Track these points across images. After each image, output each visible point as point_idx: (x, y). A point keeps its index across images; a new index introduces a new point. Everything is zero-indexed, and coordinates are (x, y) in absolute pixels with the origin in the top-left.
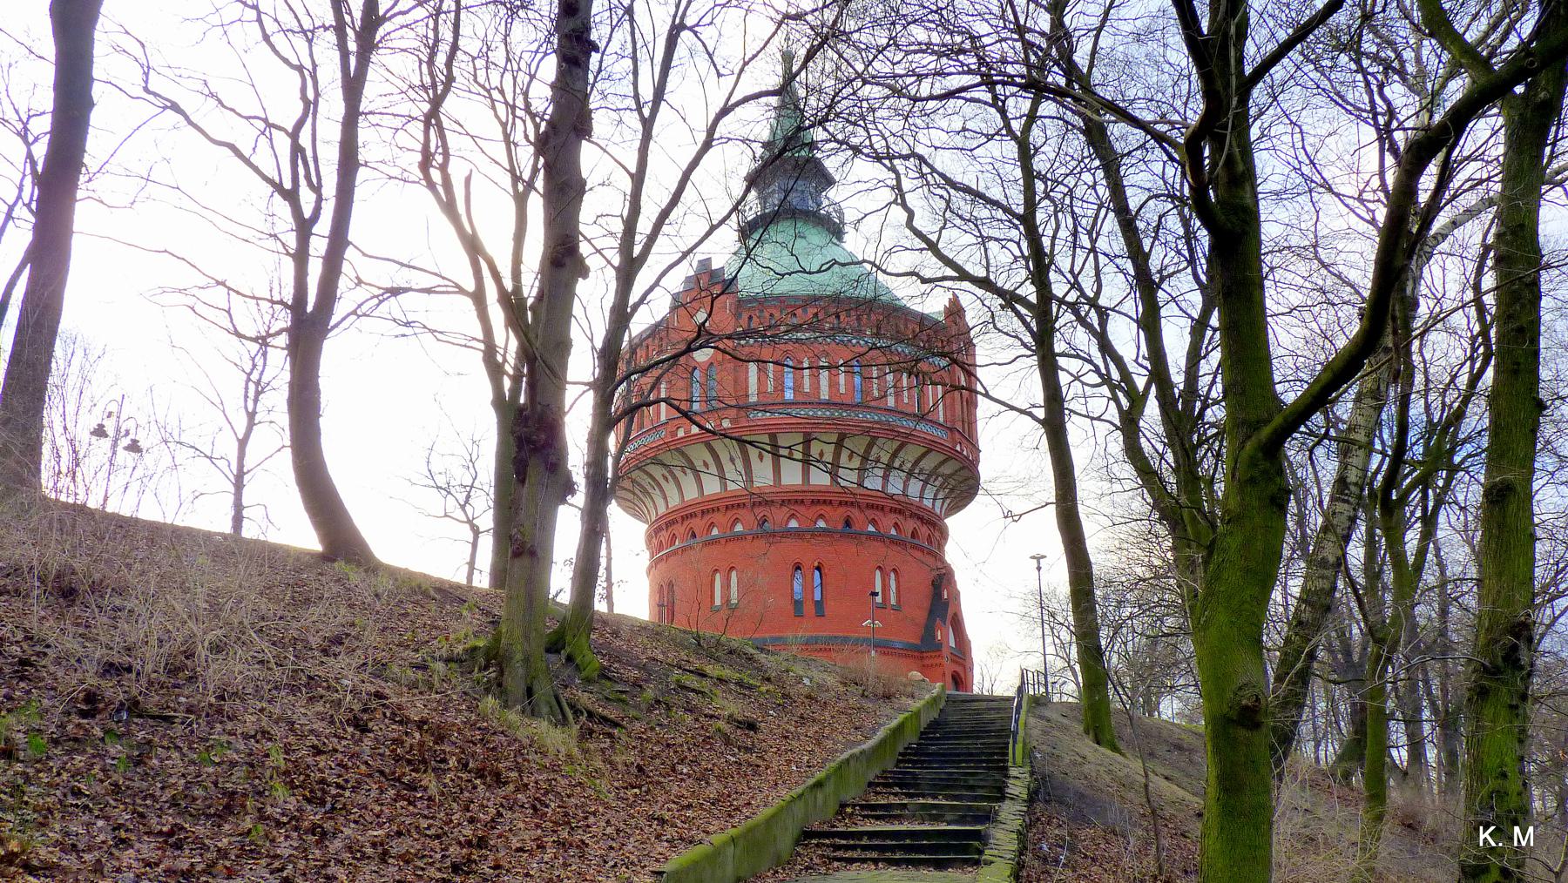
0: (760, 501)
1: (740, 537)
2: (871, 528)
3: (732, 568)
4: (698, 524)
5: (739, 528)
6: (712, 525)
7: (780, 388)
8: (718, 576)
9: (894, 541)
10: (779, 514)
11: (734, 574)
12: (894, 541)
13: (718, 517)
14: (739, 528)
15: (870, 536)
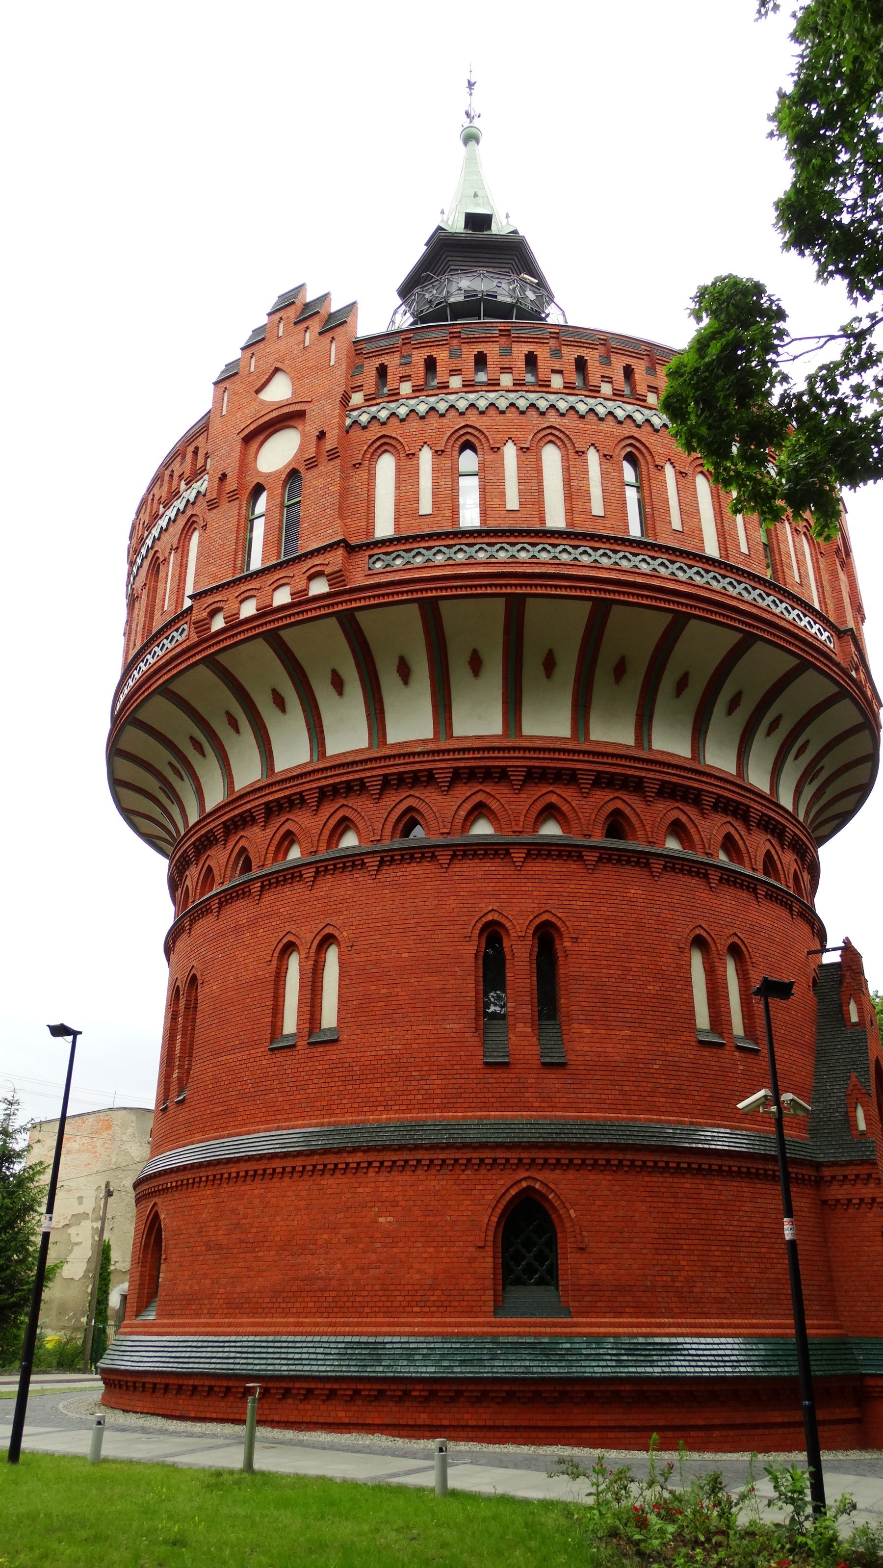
0: (399, 774)
1: (352, 862)
2: (672, 845)
3: (327, 940)
4: (257, 838)
5: (350, 841)
6: (289, 839)
7: (448, 499)
8: (294, 963)
9: (730, 878)
10: (440, 807)
11: (332, 956)
12: (730, 878)
13: (303, 821)
14: (350, 841)
15: (672, 863)
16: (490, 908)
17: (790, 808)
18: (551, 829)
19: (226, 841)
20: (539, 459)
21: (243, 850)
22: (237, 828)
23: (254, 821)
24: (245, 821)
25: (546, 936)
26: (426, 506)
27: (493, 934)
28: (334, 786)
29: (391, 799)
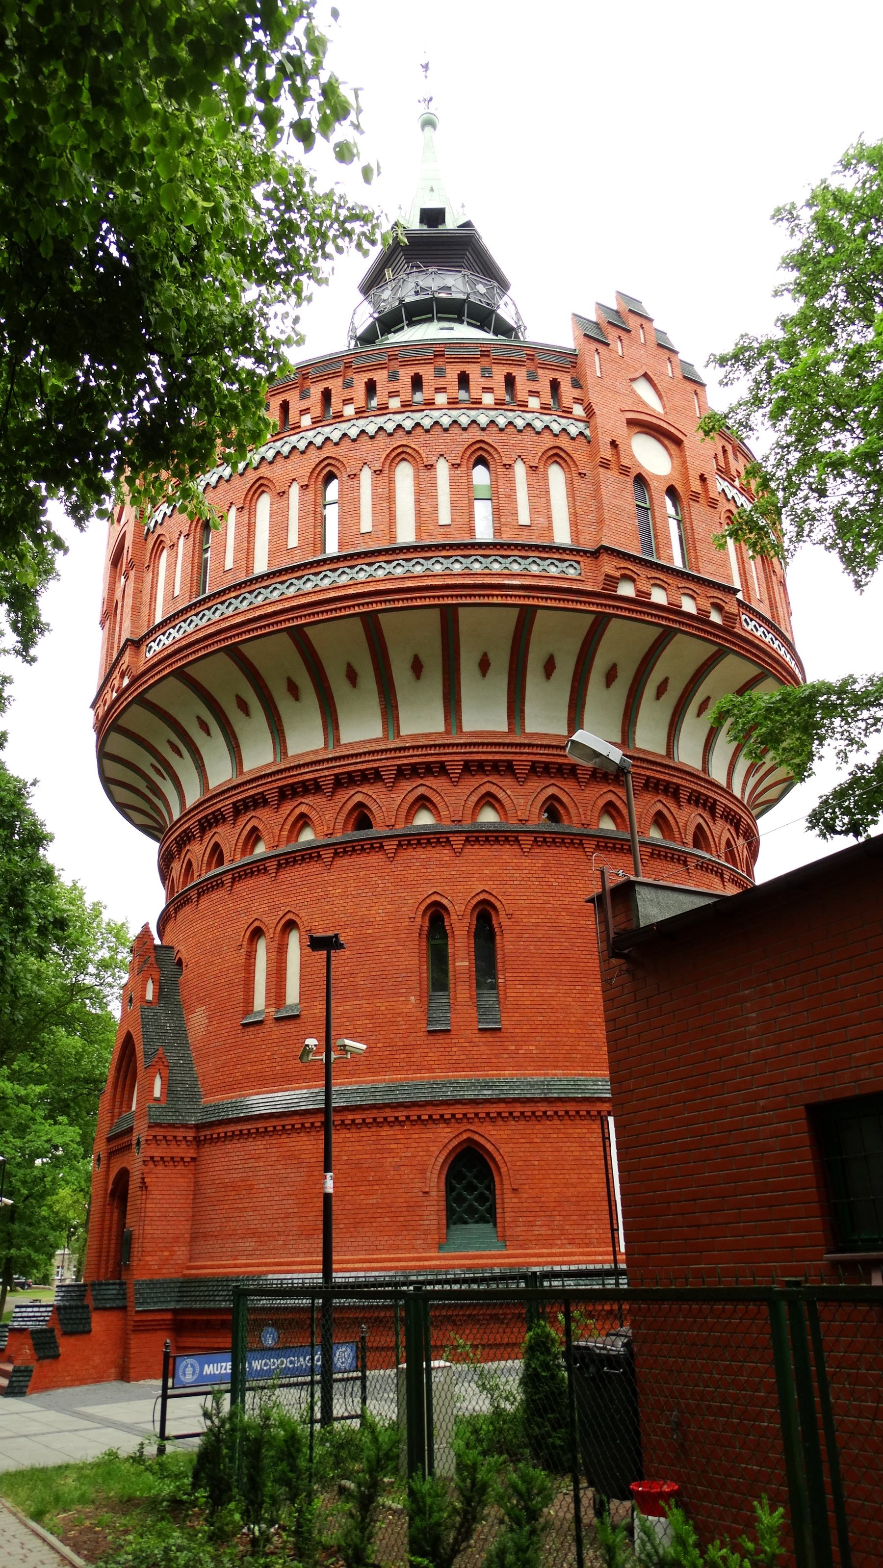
13: (267, 819)
16: (434, 890)
17: (723, 783)
18: (489, 816)
19: (202, 837)
20: (391, 481)
21: (217, 846)
22: (210, 826)
23: (224, 819)
24: (217, 819)
25: (485, 915)
26: (293, 541)
27: (436, 915)
28: (293, 787)
29: (342, 796)
